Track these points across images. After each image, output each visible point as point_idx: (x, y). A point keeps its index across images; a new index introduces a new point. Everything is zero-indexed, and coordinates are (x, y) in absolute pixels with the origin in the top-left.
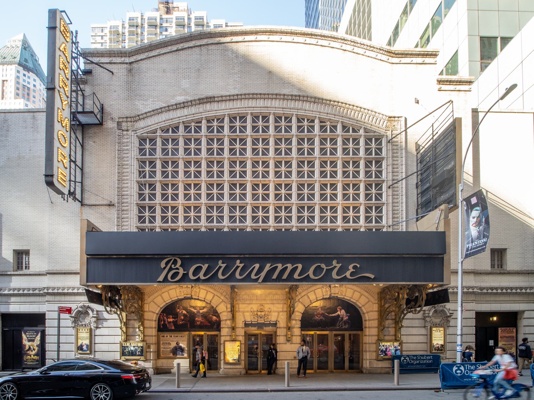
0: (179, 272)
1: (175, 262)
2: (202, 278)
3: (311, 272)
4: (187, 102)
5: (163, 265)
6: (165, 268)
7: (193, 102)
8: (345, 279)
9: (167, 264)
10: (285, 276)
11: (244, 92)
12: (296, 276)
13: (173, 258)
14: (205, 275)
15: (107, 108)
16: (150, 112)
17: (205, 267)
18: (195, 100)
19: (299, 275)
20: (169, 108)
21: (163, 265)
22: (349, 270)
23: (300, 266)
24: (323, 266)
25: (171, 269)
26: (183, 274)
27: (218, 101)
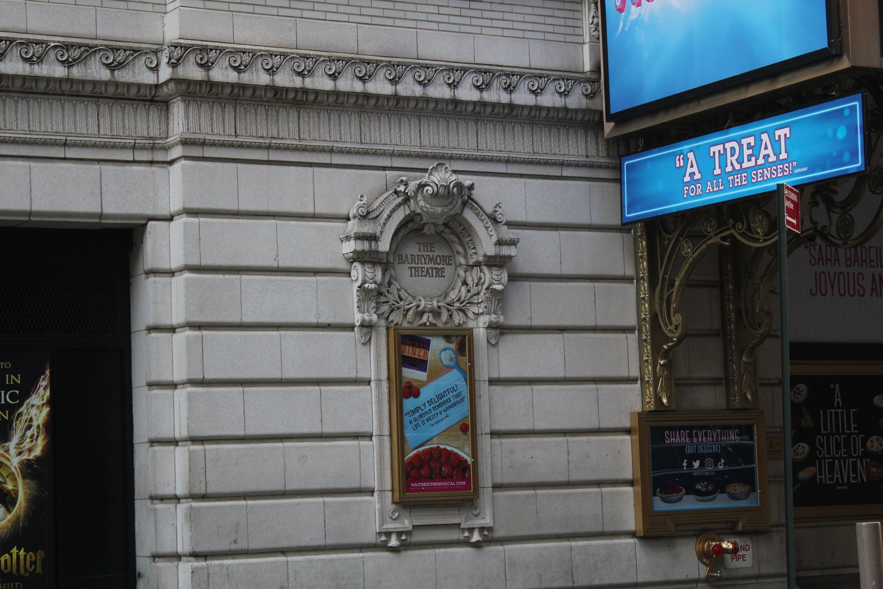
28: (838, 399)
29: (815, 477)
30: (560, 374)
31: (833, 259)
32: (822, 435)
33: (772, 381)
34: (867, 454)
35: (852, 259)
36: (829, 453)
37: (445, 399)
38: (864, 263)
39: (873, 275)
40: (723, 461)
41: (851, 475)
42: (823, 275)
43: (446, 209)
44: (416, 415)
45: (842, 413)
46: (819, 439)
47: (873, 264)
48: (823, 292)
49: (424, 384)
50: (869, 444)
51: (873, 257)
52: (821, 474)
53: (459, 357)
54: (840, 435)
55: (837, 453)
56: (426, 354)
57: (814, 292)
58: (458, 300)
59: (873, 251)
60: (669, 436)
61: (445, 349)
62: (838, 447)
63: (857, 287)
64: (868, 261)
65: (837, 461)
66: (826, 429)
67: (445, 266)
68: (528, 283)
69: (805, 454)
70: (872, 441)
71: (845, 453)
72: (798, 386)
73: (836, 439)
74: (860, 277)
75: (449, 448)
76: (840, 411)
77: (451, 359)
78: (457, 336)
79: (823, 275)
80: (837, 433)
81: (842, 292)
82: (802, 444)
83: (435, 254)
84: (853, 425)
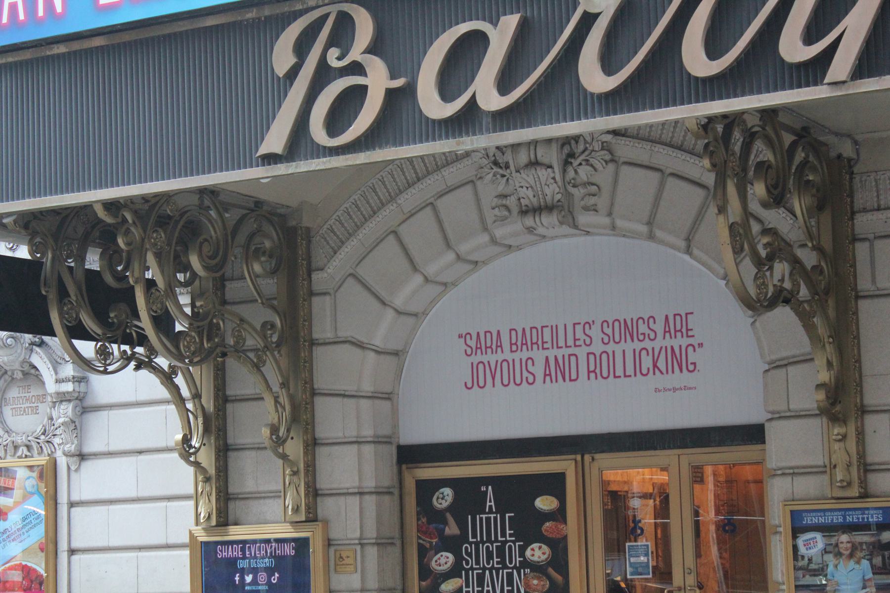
0: (364, 89)
1: (343, 31)
2: (492, 101)
5: (282, 58)
6: (293, 74)
9: (302, 48)
13: (334, 9)
14: (504, 84)
17: (501, 34)
21: (282, 58)
25: (323, 75)
26: (390, 94)
28: (490, 503)
29: (461, 588)
30: (133, 494)
31: (494, 347)
32: (471, 544)
33: (350, 491)
34: (525, 564)
35: (519, 343)
36: (478, 563)
37: (27, 521)
38: (535, 347)
39: (547, 358)
40: (277, 575)
41: (506, 588)
42: (481, 366)
43: (11, 358)
44: (5, 536)
45: (495, 518)
46: (466, 548)
47: (545, 346)
48: (481, 384)
49: (11, 509)
50: (528, 553)
51: (547, 338)
52: (467, 586)
53: (40, 484)
54: (492, 543)
55: (488, 563)
56: (13, 483)
57: (469, 385)
58: (44, 434)
59: (547, 332)
60: (221, 551)
61: (28, 478)
62: (490, 556)
63: (525, 374)
64: (684, 330)
65: (487, 572)
66: (474, 536)
67: (39, 404)
68: (106, 412)
69: (449, 564)
70: (533, 550)
71: (498, 563)
72: (442, 490)
73: (488, 547)
74: (530, 362)
75: (29, 564)
76: (492, 516)
77: (33, 486)
78: (38, 466)
79: (481, 366)
80: (489, 540)
81: (506, 382)
82: (444, 554)
83: (31, 394)
84: (508, 532)
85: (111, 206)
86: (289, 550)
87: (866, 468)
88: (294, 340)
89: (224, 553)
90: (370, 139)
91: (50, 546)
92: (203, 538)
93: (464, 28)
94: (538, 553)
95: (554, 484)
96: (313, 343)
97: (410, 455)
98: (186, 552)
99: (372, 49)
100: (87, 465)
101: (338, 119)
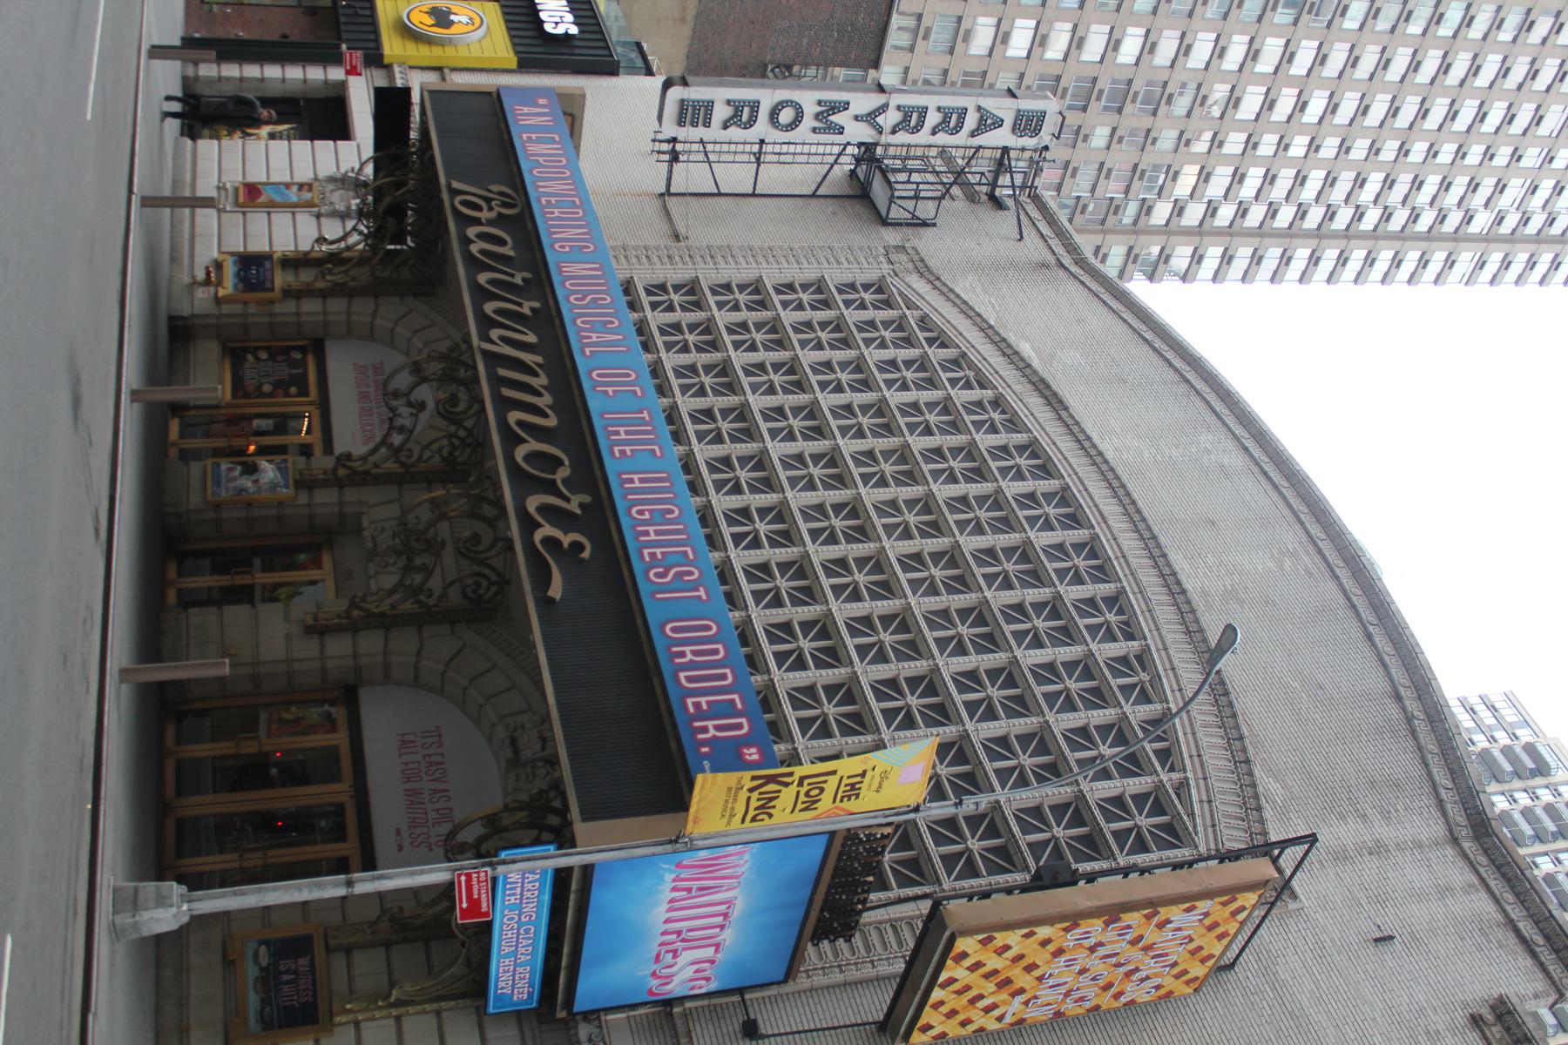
2: (474, 248)
3: (534, 445)
4: (1022, 359)
7: (1028, 371)
8: (529, 525)
9: (501, 194)
10: (506, 392)
11: (1119, 471)
12: (514, 416)
14: (482, 252)
15: (928, 233)
16: (958, 296)
17: (507, 251)
18: (1035, 372)
19: (520, 423)
20: (986, 328)
22: (566, 533)
23: (552, 422)
24: (563, 473)
27: (1060, 418)
34: (261, 384)
85: (432, 157)
86: (268, 285)
87: (310, 489)
88: (378, 289)
89: (267, 264)
90: (456, 212)
91: (272, 205)
92: (275, 256)
93: (509, 239)
94: (267, 388)
95: (304, 392)
96: (376, 297)
97: (318, 347)
98: (267, 249)
99: (500, 214)
100: (314, 220)
101: (466, 203)
